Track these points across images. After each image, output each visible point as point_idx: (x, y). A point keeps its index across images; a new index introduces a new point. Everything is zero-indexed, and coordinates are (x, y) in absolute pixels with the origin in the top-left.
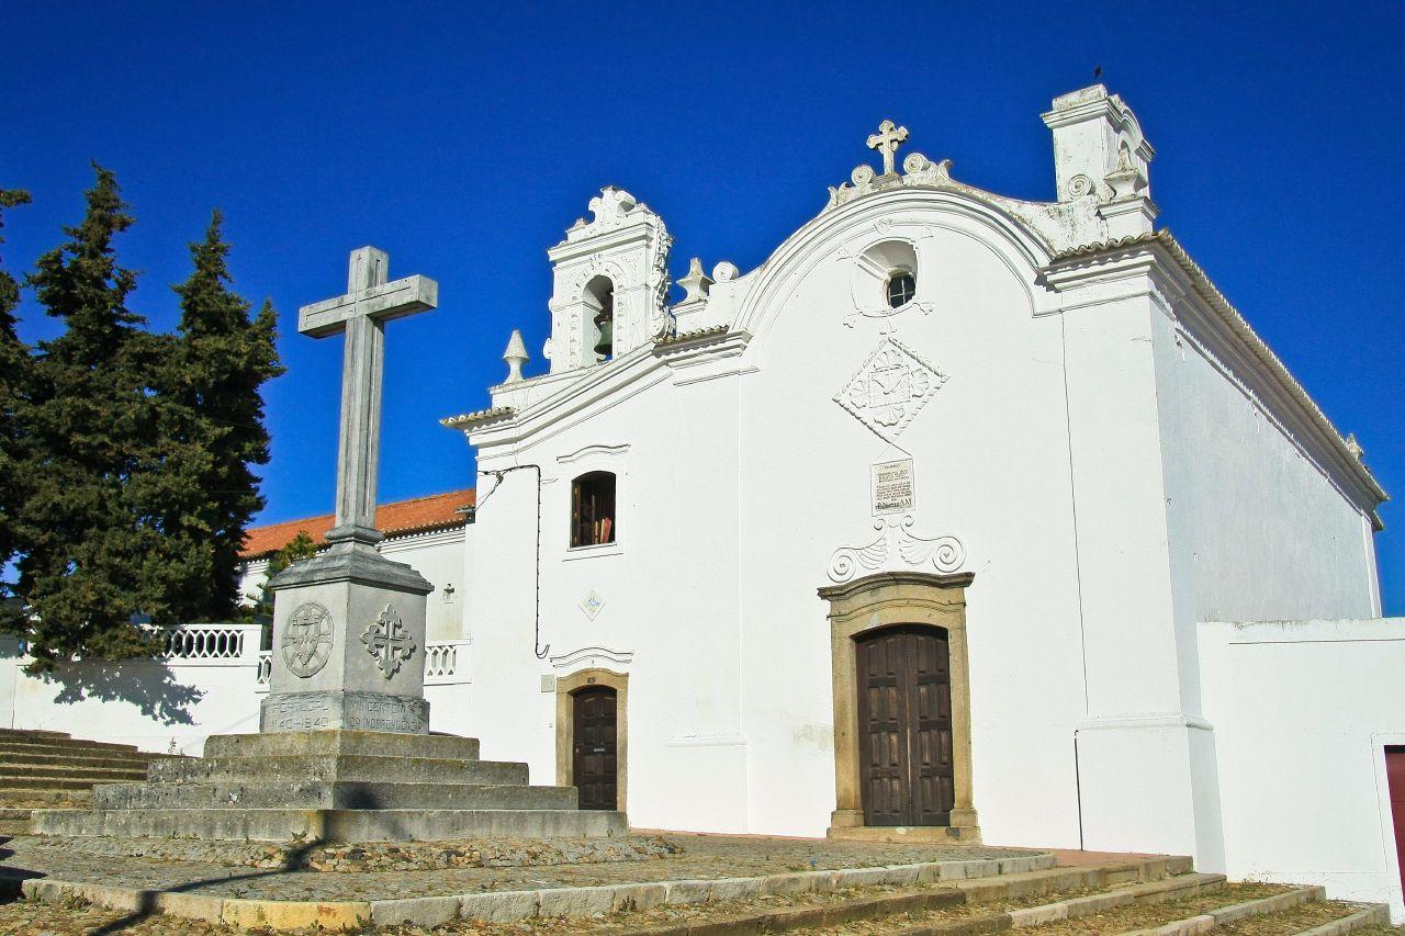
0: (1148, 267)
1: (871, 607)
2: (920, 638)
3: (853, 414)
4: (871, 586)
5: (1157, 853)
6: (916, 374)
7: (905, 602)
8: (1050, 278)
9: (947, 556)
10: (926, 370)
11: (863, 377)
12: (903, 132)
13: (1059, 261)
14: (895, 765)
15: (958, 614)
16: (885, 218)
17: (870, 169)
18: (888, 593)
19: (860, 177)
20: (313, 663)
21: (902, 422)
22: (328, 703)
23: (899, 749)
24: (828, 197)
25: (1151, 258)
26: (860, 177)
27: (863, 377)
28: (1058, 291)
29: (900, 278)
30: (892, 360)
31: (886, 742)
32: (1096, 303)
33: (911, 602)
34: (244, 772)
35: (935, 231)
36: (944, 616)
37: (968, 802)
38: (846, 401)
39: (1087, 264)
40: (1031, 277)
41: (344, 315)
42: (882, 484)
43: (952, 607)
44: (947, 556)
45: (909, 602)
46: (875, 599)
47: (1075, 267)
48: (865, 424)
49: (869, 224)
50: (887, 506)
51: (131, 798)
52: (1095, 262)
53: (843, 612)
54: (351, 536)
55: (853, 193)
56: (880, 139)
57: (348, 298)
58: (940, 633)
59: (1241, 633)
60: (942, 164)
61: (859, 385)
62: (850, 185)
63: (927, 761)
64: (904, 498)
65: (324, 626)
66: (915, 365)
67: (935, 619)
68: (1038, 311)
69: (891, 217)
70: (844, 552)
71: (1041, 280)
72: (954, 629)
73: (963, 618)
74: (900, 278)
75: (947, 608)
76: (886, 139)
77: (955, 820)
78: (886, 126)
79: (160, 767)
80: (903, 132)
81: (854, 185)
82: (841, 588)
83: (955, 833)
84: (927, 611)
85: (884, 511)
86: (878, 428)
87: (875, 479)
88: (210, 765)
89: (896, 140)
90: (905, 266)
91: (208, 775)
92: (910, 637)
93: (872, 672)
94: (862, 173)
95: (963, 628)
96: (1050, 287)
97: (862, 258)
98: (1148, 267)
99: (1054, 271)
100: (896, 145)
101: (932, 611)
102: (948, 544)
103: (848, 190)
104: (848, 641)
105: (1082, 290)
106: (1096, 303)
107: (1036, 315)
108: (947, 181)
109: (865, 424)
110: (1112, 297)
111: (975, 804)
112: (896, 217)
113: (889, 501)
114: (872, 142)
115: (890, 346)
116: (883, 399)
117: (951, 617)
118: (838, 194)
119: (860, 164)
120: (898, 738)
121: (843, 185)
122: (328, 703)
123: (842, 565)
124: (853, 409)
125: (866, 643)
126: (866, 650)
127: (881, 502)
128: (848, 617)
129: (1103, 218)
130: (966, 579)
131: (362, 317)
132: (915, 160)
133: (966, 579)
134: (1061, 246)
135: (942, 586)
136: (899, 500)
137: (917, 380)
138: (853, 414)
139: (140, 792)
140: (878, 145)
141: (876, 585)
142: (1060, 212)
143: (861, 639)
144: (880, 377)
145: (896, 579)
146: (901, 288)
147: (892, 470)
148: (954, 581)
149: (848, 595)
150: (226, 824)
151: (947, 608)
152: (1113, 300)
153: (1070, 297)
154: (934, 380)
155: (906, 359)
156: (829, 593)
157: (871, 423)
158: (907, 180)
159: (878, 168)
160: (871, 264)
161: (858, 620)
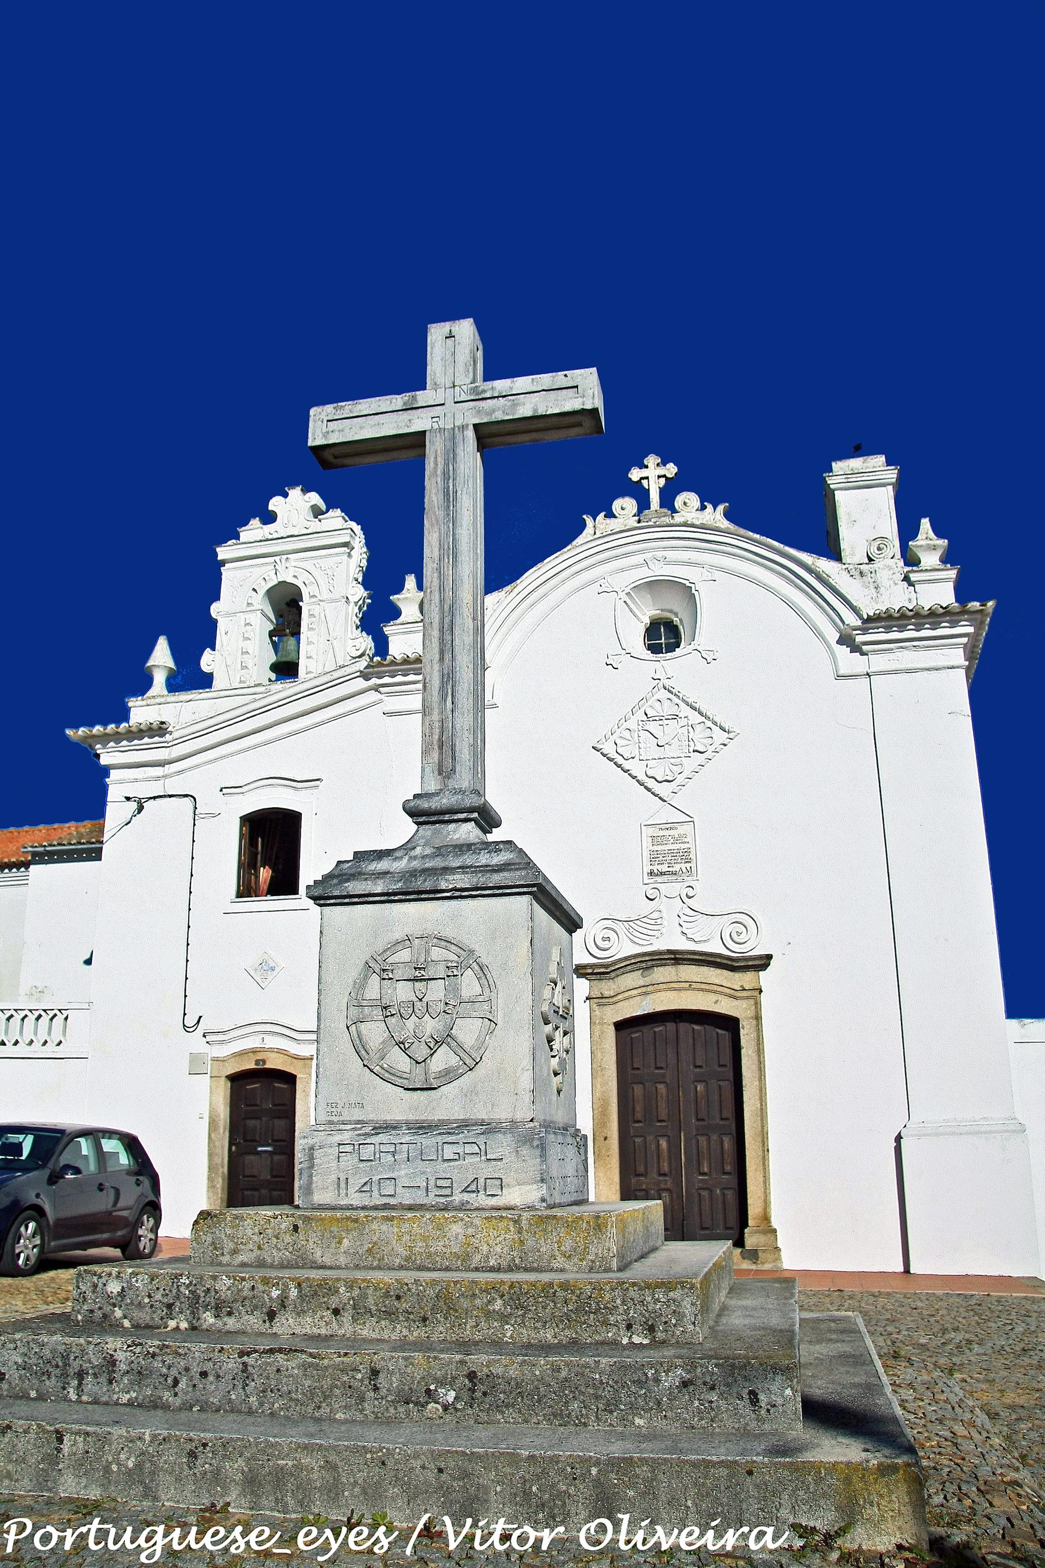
0: (965, 640)
1: (644, 989)
2: (696, 1027)
3: (619, 766)
4: (644, 965)
5: (997, 1274)
6: (698, 728)
7: (687, 985)
8: (859, 639)
9: (739, 934)
10: (709, 724)
11: (632, 724)
12: (671, 470)
13: (870, 622)
14: (665, 1175)
15: (752, 1002)
16: (659, 554)
17: (634, 502)
18: (663, 973)
19: (623, 509)
20: (443, 1059)
21: (680, 779)
22: (502, 1145)
23: (670, 1157)
24: (583, 526)
25: (971, 630)
26: (623, 509)
27: (632, 724)
28: (863, 654)
29: (659, 624)
30: (668, 709)
31: (653, 1147)
32: (908, 671)
33: (694, 985)
34: (390, 1314)
35: (717, 575)
36: (735, 1002)
37: (766, 1218)
38: (609, 748)
39: (902, 629)
40: (833, 636)
41: (418, 422)
42: (656, 848)
43: (745, 994)
44: (739, 934)
45: (691, 986)
46: (647, 980)
47: (888, 629)
48: (634, 777)
49: (639, 559)
50: (662, 874)
51: (81, 1375)
52: (927, 626)
53: (607, 993)
54: (471, 810)
55: (613, 524)
56: (644, 473)
57: (423, 397)
58: (730, 1024)
59: (1023, 1031)
60: (721, 508)
61: (627, 734)
62: (610, 515)
63: (706, 1170)
64: (683, 866)
65: (469, 984)
66: (695, 718)
67: (725, 1007)
68: (842, 672)
69: (665, 553)
70: (608, 923)
71: (846, 640)
72: (747, 1018)
73: (757, 1005)
74: (659, 624)
75: (738, 994)
76: (653, 473)
77: (751, 1240)
78: (652, 460)
79: (114, 1287)
80: (671, 470)
81: (615, 517)
82: (602, 966)
83: (753, 1255)
84: (714, 997)
85: (659, 879)
86: (651, 783)
87: (647, 843)
88: (275, 1293)
89: (664, 476)
90: (671, 611)
91: (271, 1315)
92: (683, 1026)
93: (635, 1066)
94: (625, 506)
95: (758, 1018)
96: (856, 648)
97: (628, 594)
98: (965, 640)
99: (865, 631)
100: (663, 481)
101: (720, 997)
102: (743, 919)
103: (608, 521)
104: (611, 1031)
105: (891, 656)
106: (908, 671)
107: (839, 677)
108: (725, 524)
109: (634, 777)
110: (927, 666)
111: (775, 1223)
112: (671, 555)
113: (664, 868)
114: (635, 475)
115: (663, 694)
116: (659, 752)
117: (744, 1004)
118: (596, 526)
119: (623, 495)
120: (669, 1142)
121: (602, 514)
122: (502, 1145)
123: (604, 939)
124: (620, 760)
125: (628, 1031)
126: (628, 1039)
127: (655, 868)
128: (614, 999)
129: (911, 584)
130: (763, 962)
131: (463, 428)
132: (688, 501)
133: (763, 962)
134: (868, 611)
135: (733, 969)
136: (676, 868)
137: (699, 735)
138: (619, 766)
139: (112, 1362)
140: (642, 478)
141: (650, 963)
142: (861, 573)
143: (621, 1026)
144: (652, 726)
145: (676, 958)
146: (663, 636)
147: (666, 833)
148: (750, 963)
149: (613, 974)
150: (527, 1494)
151: (738, 994)
152: (928, 669)
153: (878, 662)
154: (720, 736)
155: (685, 710)
156: (590, 971)
157: (642, 777)
158: (678, 518)
159: (643, 504)
160: (635, 603)
161: (625, 1003)
